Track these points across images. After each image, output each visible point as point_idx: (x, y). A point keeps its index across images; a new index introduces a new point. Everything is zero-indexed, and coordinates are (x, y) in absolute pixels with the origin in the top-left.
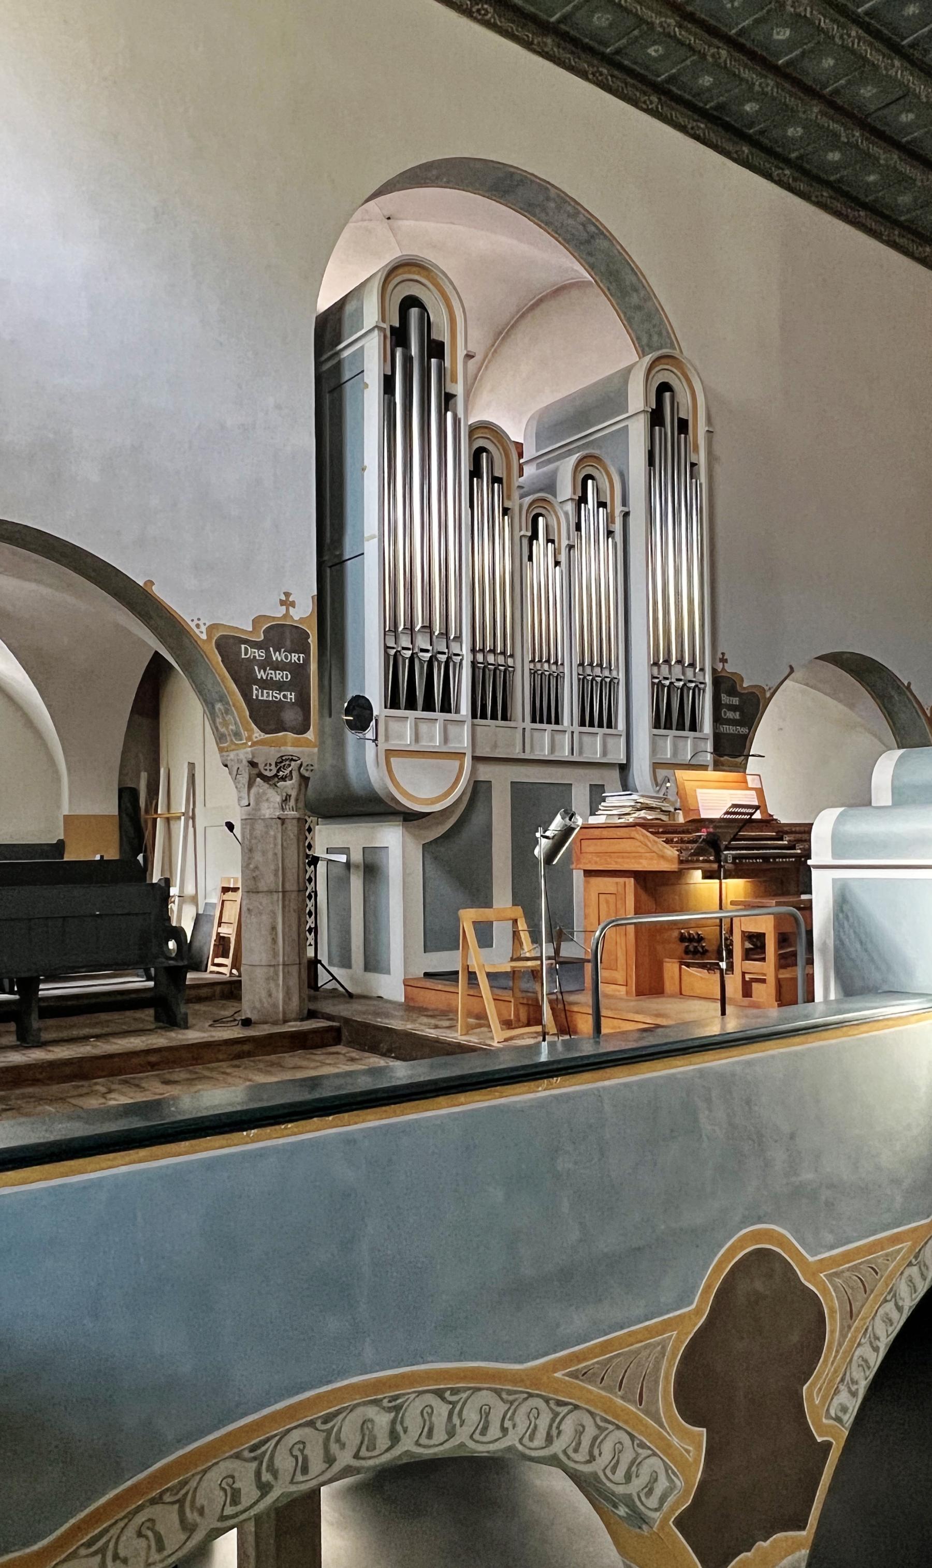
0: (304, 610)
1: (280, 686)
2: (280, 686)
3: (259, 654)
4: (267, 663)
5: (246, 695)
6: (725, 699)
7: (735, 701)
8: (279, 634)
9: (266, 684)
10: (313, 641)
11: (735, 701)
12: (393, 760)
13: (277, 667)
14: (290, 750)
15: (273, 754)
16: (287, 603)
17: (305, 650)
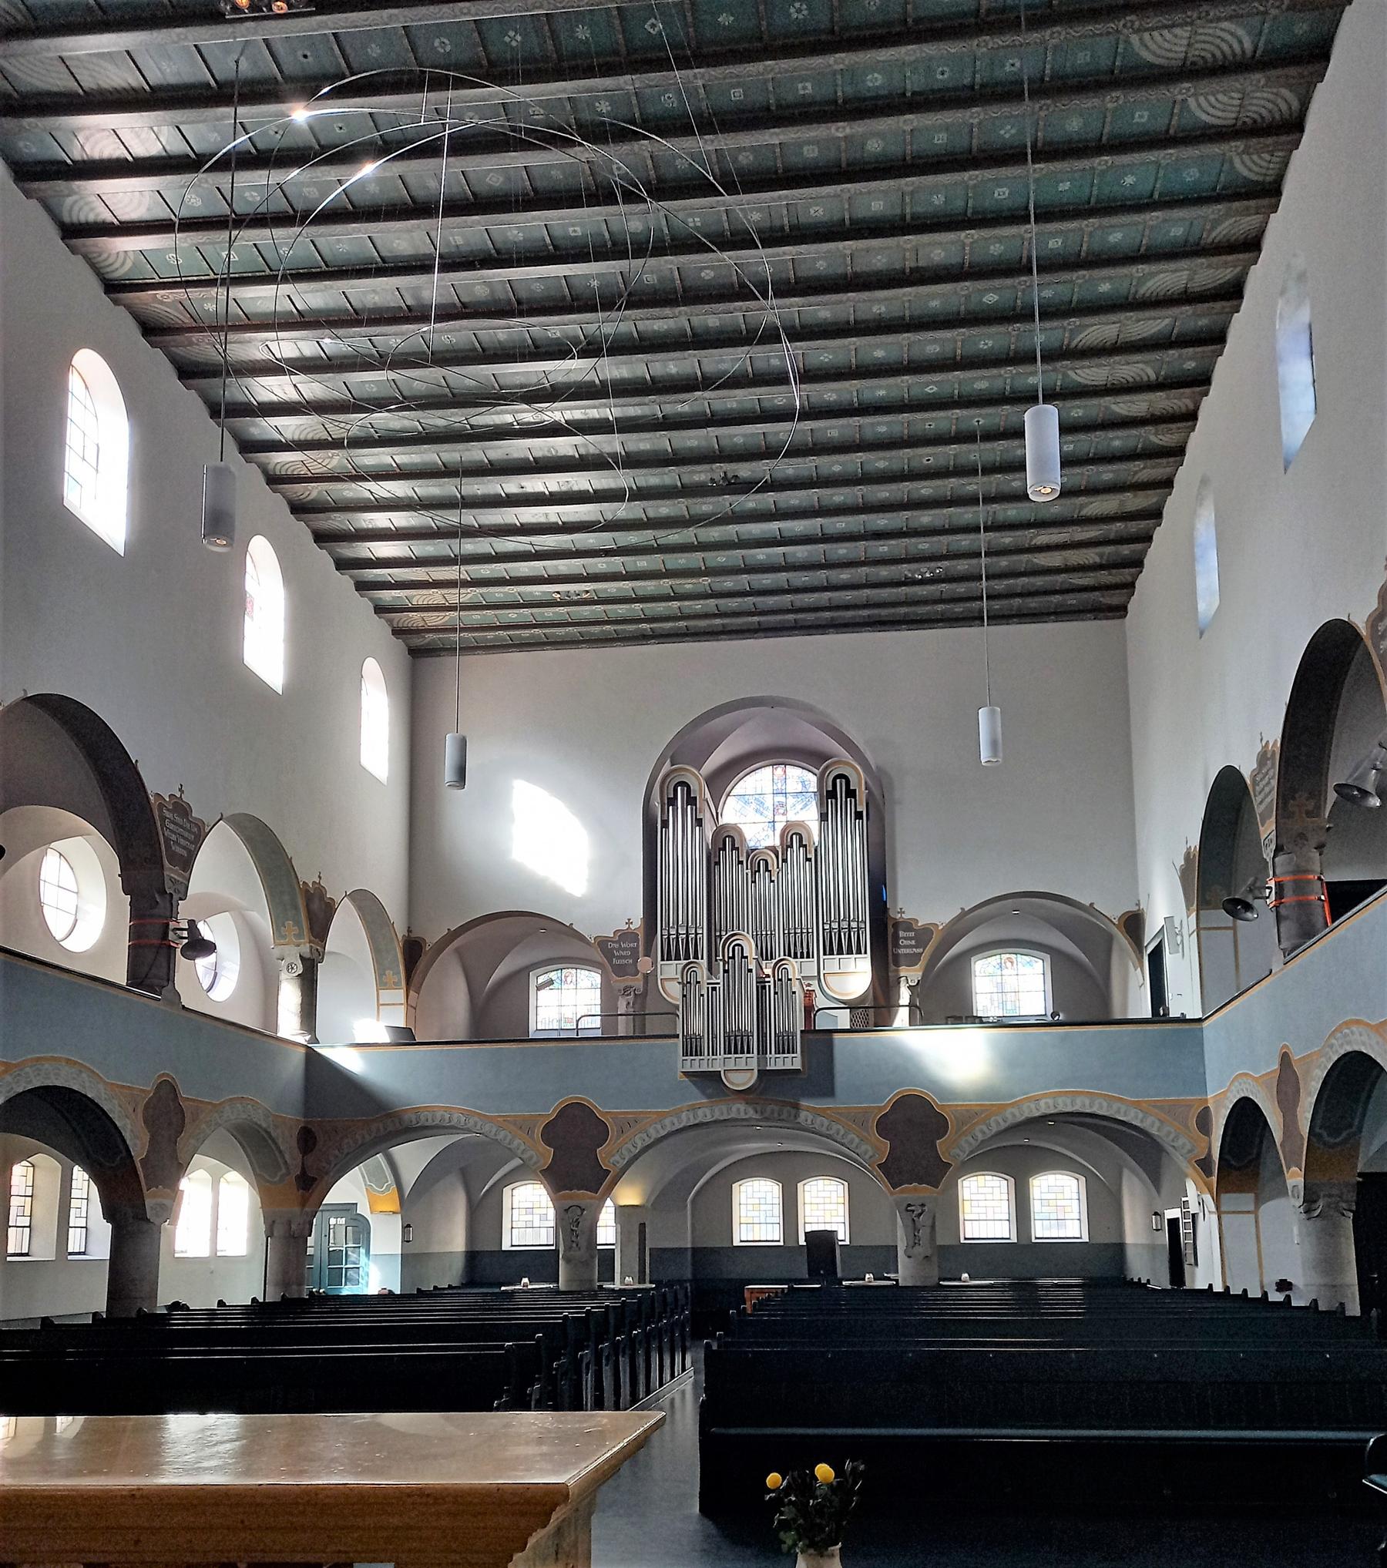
0: (637, 922)
1: (625, 957)
2: (625, 957)
3: (616, 946)
4: (620, 948)
5: (610, 962)
6: (901, 934)
7: (912, 934)
8: (625, 936)
9: (619, 958)
10: (641, 937)
11: (912, 934)
12: (666, 984)
13: (624, 949)
14: (629, 984)
15: (622, 986)
16: (629, 922)
17: (637, 941)
